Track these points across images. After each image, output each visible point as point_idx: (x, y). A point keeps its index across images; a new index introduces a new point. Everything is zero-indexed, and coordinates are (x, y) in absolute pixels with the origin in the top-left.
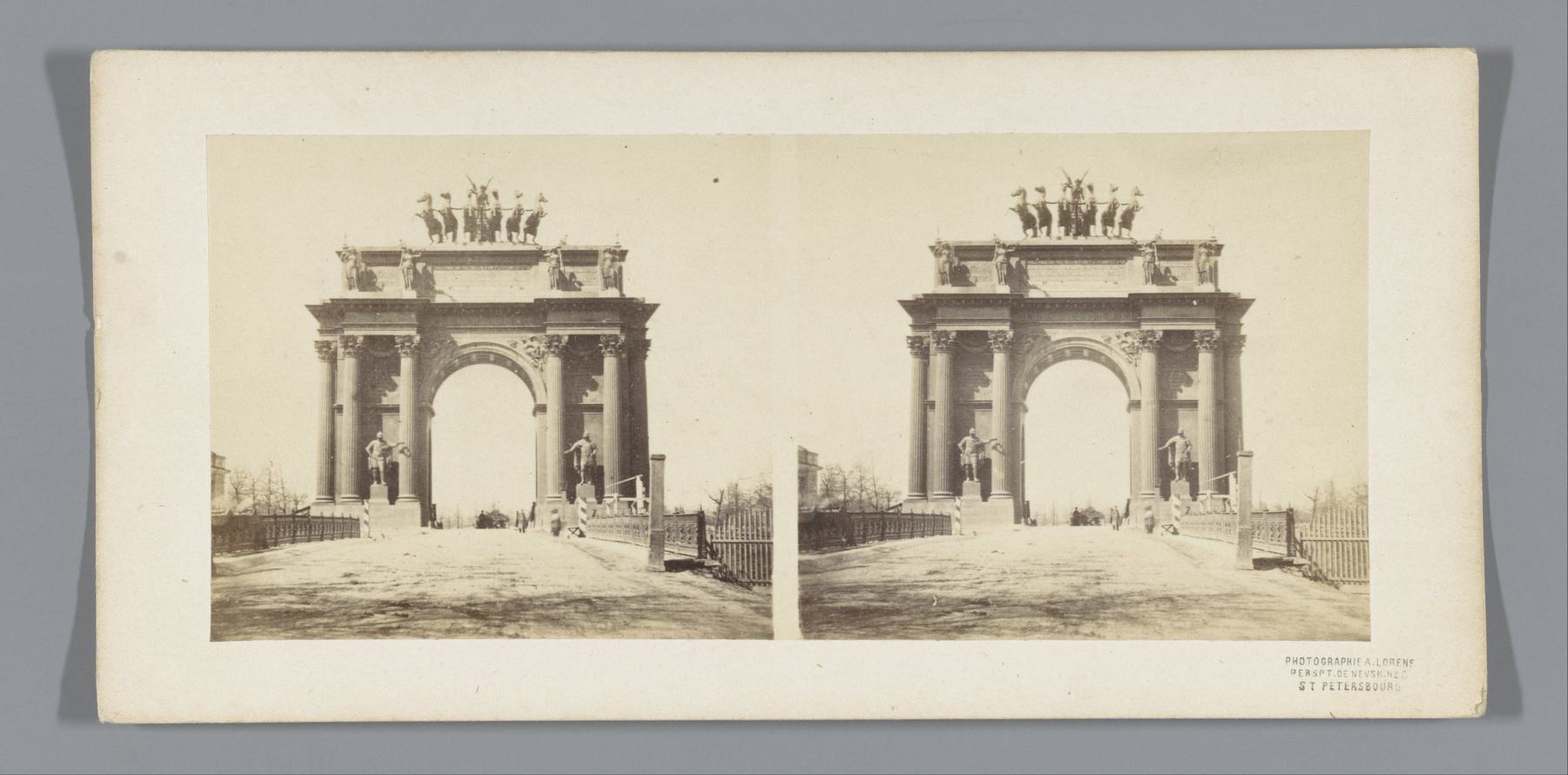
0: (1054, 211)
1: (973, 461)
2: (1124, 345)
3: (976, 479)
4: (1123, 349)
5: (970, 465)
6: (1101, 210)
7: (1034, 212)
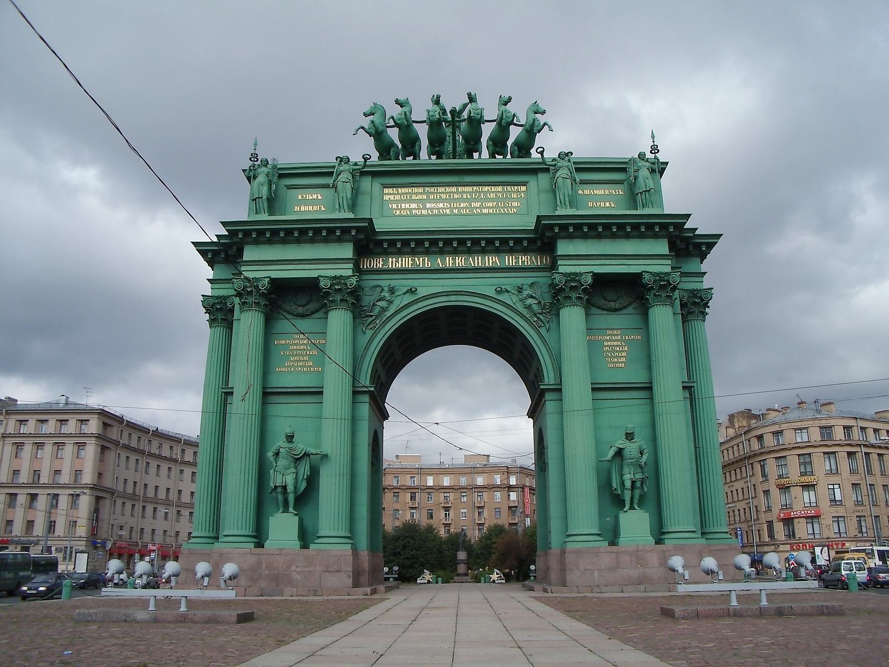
0: (422, 131)
1: (290, 480)
2: (529, 301)
3: (291, 509)
4: (529, 307)
5: (285, 488)
6: (487, 130)
7: (394, 134)
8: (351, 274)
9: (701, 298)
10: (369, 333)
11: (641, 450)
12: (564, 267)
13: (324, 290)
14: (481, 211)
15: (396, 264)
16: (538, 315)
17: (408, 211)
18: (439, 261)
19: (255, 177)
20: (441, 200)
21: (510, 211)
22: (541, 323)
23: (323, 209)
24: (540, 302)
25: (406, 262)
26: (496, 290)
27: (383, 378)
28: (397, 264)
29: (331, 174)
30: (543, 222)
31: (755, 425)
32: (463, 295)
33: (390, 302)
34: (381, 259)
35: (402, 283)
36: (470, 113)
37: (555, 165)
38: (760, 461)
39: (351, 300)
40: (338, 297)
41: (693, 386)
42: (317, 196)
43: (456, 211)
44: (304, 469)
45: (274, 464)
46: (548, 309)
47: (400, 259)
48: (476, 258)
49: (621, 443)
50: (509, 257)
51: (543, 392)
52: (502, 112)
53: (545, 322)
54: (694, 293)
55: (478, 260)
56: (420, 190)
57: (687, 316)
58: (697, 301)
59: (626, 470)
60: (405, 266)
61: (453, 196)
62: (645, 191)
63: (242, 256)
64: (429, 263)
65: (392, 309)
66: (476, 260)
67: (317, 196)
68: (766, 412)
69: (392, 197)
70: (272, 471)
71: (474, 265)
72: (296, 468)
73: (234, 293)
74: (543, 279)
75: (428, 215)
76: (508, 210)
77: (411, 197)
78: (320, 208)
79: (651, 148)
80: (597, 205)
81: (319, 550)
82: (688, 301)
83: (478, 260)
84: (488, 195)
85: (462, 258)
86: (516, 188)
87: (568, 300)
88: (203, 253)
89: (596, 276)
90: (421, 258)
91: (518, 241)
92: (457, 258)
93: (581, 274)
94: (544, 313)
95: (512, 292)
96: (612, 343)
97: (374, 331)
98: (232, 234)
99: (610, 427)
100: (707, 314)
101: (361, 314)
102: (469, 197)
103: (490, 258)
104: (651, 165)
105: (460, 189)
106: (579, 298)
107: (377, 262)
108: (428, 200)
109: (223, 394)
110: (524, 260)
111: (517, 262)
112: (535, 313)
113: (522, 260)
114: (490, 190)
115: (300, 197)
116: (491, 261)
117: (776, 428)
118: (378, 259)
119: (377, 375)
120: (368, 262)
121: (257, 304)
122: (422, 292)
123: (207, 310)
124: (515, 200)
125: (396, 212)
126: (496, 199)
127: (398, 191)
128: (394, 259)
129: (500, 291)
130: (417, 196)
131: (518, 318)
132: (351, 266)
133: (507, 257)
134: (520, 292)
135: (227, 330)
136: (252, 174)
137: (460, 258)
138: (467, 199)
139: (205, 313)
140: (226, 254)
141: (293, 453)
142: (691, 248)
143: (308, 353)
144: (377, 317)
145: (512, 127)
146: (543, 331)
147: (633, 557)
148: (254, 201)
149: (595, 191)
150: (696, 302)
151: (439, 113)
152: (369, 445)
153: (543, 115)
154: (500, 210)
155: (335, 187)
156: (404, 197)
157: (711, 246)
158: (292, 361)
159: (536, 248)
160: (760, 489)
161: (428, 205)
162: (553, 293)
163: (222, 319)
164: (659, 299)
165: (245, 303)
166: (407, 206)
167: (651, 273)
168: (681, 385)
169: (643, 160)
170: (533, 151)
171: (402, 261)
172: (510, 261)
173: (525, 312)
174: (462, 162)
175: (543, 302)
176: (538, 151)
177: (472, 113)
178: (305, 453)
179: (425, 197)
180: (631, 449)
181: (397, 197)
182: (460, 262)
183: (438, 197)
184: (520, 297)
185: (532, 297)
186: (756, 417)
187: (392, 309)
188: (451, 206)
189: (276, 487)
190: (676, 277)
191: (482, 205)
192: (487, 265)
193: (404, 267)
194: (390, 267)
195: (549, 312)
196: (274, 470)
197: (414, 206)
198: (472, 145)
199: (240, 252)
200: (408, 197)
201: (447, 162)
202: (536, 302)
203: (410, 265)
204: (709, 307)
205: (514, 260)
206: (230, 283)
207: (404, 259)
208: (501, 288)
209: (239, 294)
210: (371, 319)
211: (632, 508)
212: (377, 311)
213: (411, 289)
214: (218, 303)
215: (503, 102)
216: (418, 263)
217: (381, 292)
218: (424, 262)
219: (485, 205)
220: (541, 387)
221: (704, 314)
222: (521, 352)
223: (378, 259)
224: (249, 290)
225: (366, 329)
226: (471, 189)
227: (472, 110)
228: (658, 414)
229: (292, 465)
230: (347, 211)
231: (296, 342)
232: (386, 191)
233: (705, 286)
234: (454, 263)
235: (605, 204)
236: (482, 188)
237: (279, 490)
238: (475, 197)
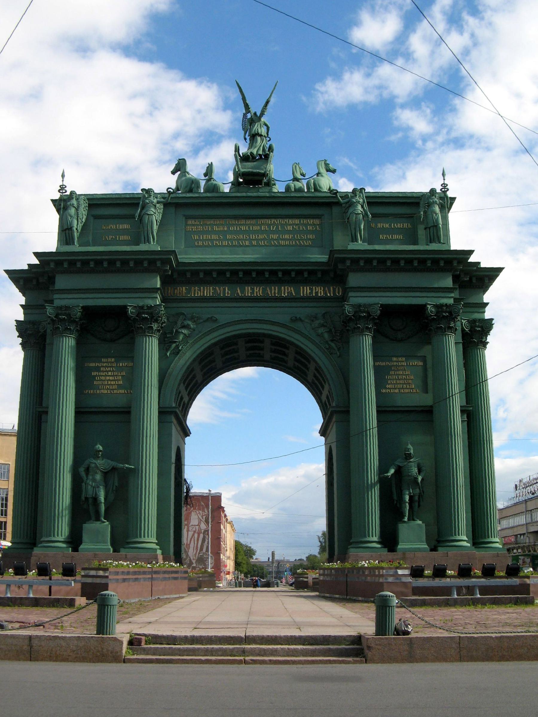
4: (320, 336)
15: (198, 292)
16: (330, 343)
24: (331, 330)
25: (208, 291)
26: (291, 319)
27: (186, 399)
28: (199, 292)
43: (254, 243)
45: (85, 478)
47: (202, 288)
48: (273, 287)
50: (303, 288)
55: (275, 289)
56: (222, 222)
61: (253, 228)
63: (53, 283)
69: (194, 229)
70: (83, 484)
71: (272, 294)
76: (303, 242)
83: (275, 289)
85: (259, 289)
90: (222, 287)
91: (311, 273)
93: (370, 305)
101: (165, 341)
111: (311, 293)
116: (286, 291)
118: (181, 288)
119: (180, 397)
122: (223, 318)
124: (311, 232)
125: (198, 243)
128: (196, 288)
129: (295, 320)
133: (301, 287)
134: (313, 321)
140: (38, 281)
142: (474, 280)
154: (295, 242)
161: (228, 237)
172: (306, 291)
185: (323, 326)
189: (86, 498)
191: (279, 236)
193: (205, 295)
196: (85, 484)
197: (214, 237)
199: (52, 280)
208: (296, 318)
210: (174, 345)
212: (181, 337)
213: (211, 318)
221: (485, 344)
222: (315, 376)
223: (181, 288)
231: (105, 365)
232: (190, 222)
233: (487, 316)
234: (252, 293)
236: (279, 221)
237: (90, 501)
238: (273, 229)
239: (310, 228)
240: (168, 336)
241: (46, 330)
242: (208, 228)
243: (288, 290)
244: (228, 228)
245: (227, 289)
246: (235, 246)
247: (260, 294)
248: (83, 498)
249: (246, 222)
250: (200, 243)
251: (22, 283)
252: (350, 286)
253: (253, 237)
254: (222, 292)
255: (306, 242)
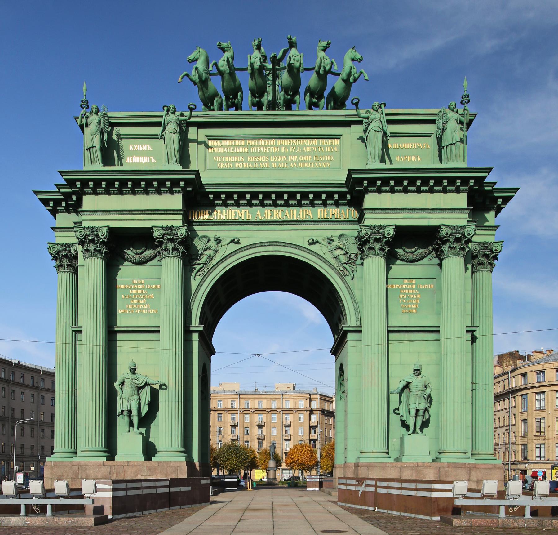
2: (338, 252)
4: (337, 257)
5: (130, 412)
8: (181, 225)
9: (491, 250)
10: (199, 279)
11: (426, 384)
12: (371, 220)
13: (158, 240)
14: (297, 165)
17: (231, 164)
18: (259, 214)
19: (87, 126)
20: (261, 154)
21: (324, 165)
22: (346, 272)
23: (153, 160)
24: (346, 253)
26: (308, 242)
29: (158, 124)
30: (354, 176)
31: (521, 365)
32: (279, 245)
33: (216, 251)
34: (207, 211)
35: (226, 234)
36: (290, 60)
37: (368, 118)
38: (521, 395)
39: (182, 249)
40: (170, 246)
41: (475, 331)
42: (147, 148)
43: (274, 165)
44: (146, 395)
46: (354, 259)
47: (224, 211)
49: (409, 377)
51: (346, 332)
52: (321, 58)
53: (350, 272)
54: (486, 246)
55: (293, 212)
56: (242, 143)
57: (477, 267)
58: (488, 253)
59: (412, 400)
60: (229, 218)
61: (272, 149)
62: (451, 144)
63: (81, 206)
64: (250, 215)
65: (218, 257)
66: (292, 213)
67: (147, 148)
68: (531, 354)
72: (139, 395)
73: (77, 241)
74: (352, 231)
75: (249, 169)
77: (233, 150)
78: (151, 159)
79: (462, 98)
80: (404, 159)
81: (160, 462)
82: (479, 253)
83: (293, 212)
84: (304, 148)
86: (330, 141)
87: (372, 252)
88: (45, 202)
89: (398, 229)
90: (243, 211)
92: (275, 211)
94: (350, 263)
95: (322, 243)
96: (407, 291)
97: (202, 277)
98: (71, 183)
99: (401, 364)
100: (495, 265)
102: (287, 150)
103: (304, 211)
104: (460, 116)
105: (279, 142)
106: (381, 249)
107: (203, 213)
108: (249, 154)
109: (74, 333)
110: (333, 212)
112: (342, 263)
113: (332, 212)
114: (306, 143)
115: (131, 148)
117: (539, 367)
120: (196, 214)
121: (99, 251)
123: (54, 257)
126: (312, 153)
127: (221, 143)
130: (239, 149)
131: (327, 267)
132: (181, 217)
133: (319, 210)
134: (329, 243)
135: (73, 275)
136: (84, 122)
137: (277, 211)
138: (284, 154)
139: (52, 260)
140: (67, 204)
141: (136, 382)
143: (146, 297)
144: (205, 264)
145: (329, 76)
146: (348, 279)
147: (414, 472)
148: (89, 150)
149: (403, 144)
150: (486, 254)
151: (260, 59)
152: (199, 376)
153: (359, 62)
155: (162, 137)
156: (227, 149)
157: (506, 200)
158: (132, 304)
159: (346, 202)
160: (519, 418)
162: (358, 245)
163: (68, 265)
164: (453, 251)
165: (87, 250)
166: (230, 159)
167: (448, 226)
168: (465, 329)
169: (453, 111)
170: (348, 102)
171: (226, 213)
173: (333, 262)
174: (281, 114)
175: (349, 253)
176: (354, 102)
177: (292, 59)
178: (146, 382)
179: (246, 150)
180: (417, 384)
181: (221, 150)
182: (278, 215)
183: (259, 150)
184: (329, 247)
185: (339, 248)
186: (522, 358)
187: (218, 257)
188: (270, 159)
190: (471, 229)
191: (298, 158)
192: (301, 218)
194: (215, 218)
195: (354, 263)
197: (236, 159)
198: (290, 95)
199: (79, 202)
200: (231, 150)
201: (266, 115)
202: (344, 252)
203: (233, 216)
204: (497, 259)
205: (325, 213)
206: (73, 231)
207: (228, 211)
208: (313, 240)
209: (82, 242)
211: (414, 432)
213: (234, 240)
214: (63, 250)
215: (322, 48)
216: (240, 216)
217: (208, 242)
218: (245, 213)
219: (301, 159)
220: (344, 329)
224: (90, 238)
225: (195, 275)
226: (289, 142)
227: (291, 57)
228: (443, 354)
229: (136, 392)
230: (175, 163)
235: (411, 158)
239: (328, 150)
240: (193, 257)
241: (78, 252)
242: (230, 149)
243: (306, 213)
244: (249, 149)
245: (247, 214)
246: (255, 169)
247: (279, 217)
248: (119, 410)
249: (265, 143)
250: (222, 166)
251: (51, 203)
252: (366, 207)
253: (272, 159)
254: (243, 215)
255: (325, 164)
